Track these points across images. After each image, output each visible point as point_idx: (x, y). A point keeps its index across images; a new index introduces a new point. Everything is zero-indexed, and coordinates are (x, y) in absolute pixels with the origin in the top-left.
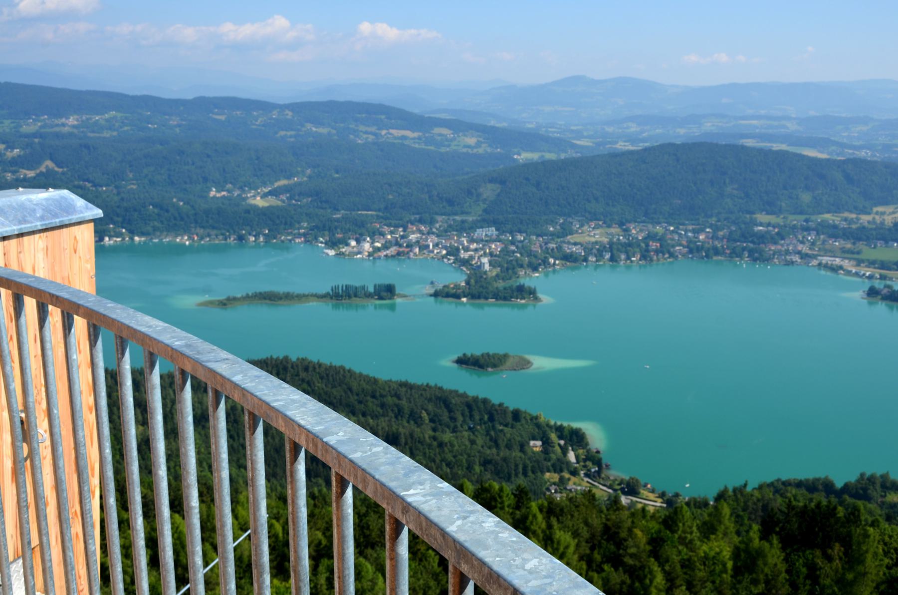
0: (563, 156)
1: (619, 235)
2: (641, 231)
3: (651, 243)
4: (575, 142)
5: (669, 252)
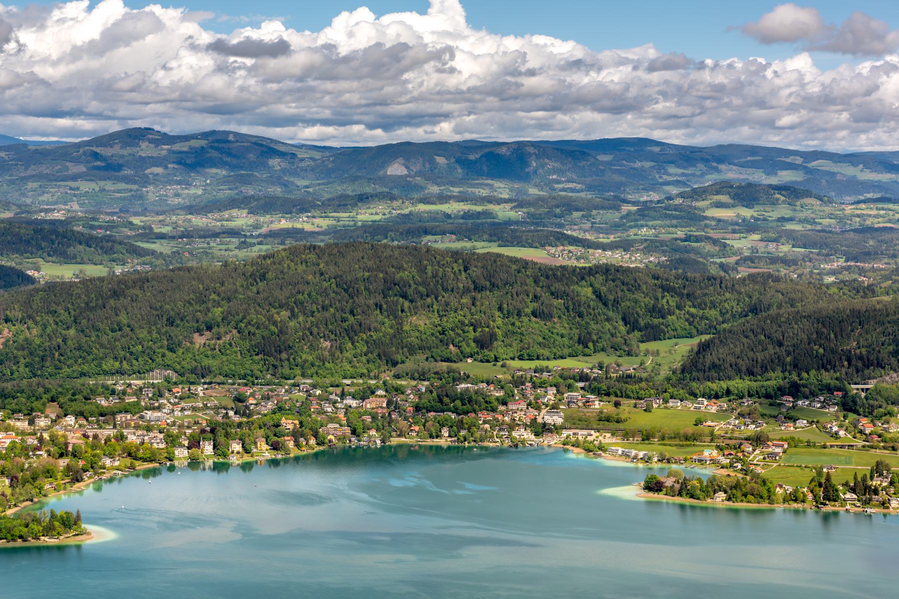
0: (118, 270)
1: (225, 408)
2: (267, 398)
3: (283, 421)
4: (139, 244)
5: (316, 435)
